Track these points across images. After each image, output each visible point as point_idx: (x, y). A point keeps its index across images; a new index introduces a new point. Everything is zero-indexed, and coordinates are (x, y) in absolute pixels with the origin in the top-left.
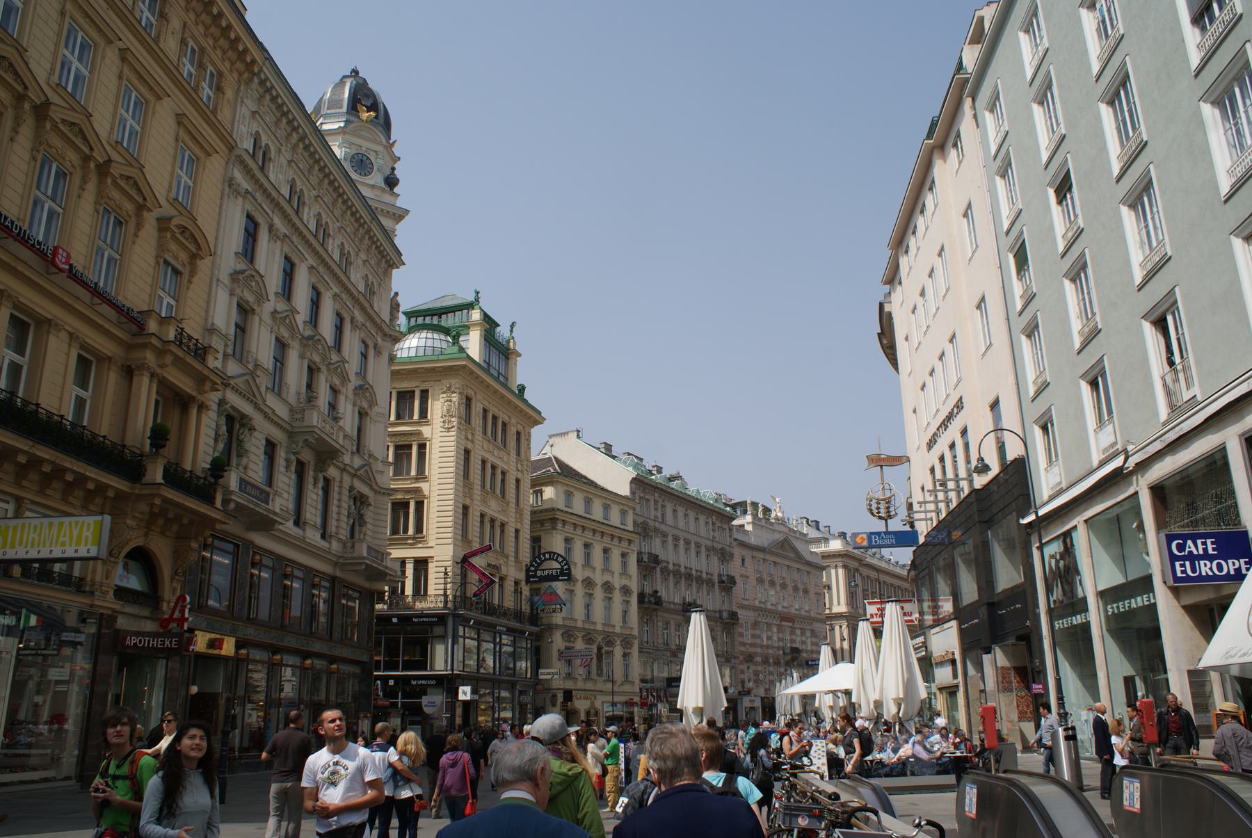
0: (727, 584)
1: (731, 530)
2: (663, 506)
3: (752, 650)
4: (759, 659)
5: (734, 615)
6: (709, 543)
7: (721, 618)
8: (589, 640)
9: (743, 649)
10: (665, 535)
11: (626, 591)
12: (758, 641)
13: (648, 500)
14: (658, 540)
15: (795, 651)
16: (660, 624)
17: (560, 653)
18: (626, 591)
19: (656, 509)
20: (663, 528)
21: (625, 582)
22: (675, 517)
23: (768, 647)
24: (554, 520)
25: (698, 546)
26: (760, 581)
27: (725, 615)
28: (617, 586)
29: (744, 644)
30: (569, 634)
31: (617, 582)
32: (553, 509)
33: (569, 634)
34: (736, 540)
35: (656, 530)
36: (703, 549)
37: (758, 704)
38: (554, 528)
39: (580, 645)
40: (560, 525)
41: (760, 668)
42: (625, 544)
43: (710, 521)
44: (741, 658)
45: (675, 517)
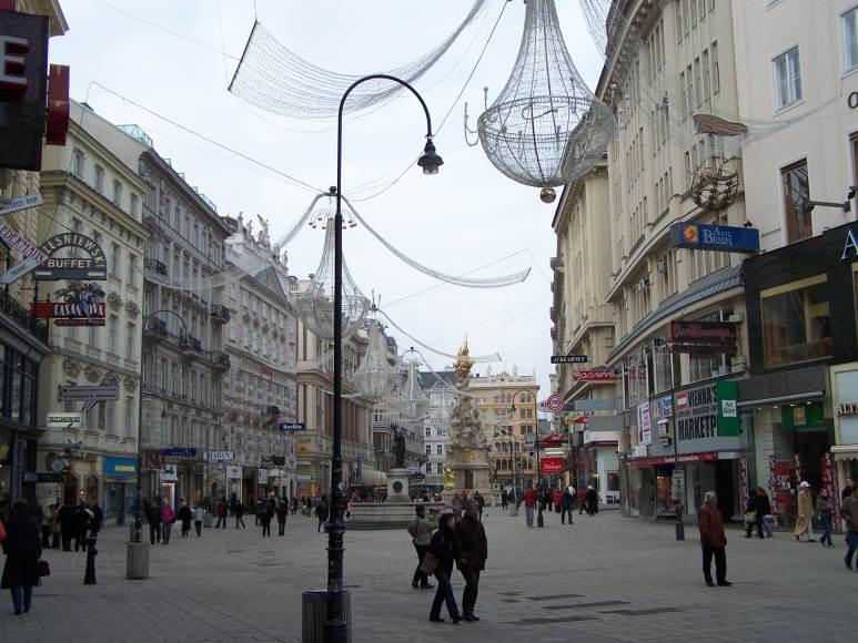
0: (220, 317)
1: (224, 249)
2: (168, 201)
3: (235, 406)
4: (241, 418)
5: (224, 359)
6: (204, 261)
7: (211, 361)
8: (93, 376)
9: (227, 403)
10: (168, 241)
11: (132, 310)
12: (242, 396)
13: (153, 188)
14: (161, 246)
15: (274, 411)
16: (159, 361)
17: (62, 391)
18: (132, 310)
19: (161, 203)
20: (168, 232)
21: (131, 297)
22: (178, 219)
23: (249, 404)
24: (61, 190)
25: (196, 262)
26: (246, 319)
27: (215, 358)
28: (124, 300)
29: (229, 399)
30: (72, 364)
31: (125, 296)
32: (63, 173)
33: (72, 364)
34: (227, 263)
35: (160, 231)
36: (200, 269)
37: (239, 475)
38: (60, 202)
39: (82, 381)
40: (67, 199)
41: (242, 430)
42: (132, 243)
43: (207, 232)
44: (226, 415)
45: (178, 219)
